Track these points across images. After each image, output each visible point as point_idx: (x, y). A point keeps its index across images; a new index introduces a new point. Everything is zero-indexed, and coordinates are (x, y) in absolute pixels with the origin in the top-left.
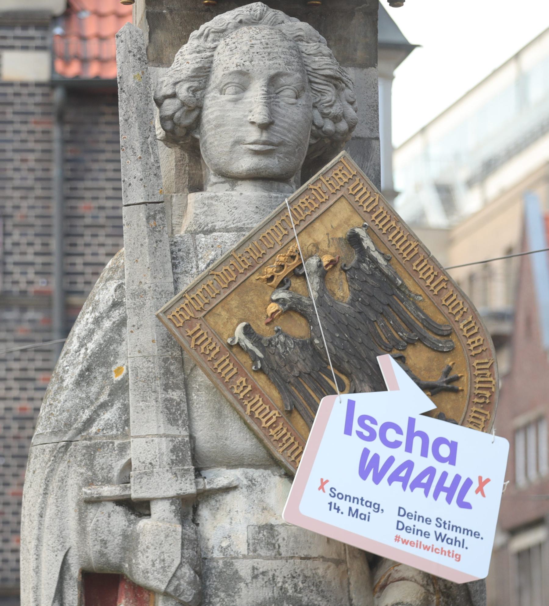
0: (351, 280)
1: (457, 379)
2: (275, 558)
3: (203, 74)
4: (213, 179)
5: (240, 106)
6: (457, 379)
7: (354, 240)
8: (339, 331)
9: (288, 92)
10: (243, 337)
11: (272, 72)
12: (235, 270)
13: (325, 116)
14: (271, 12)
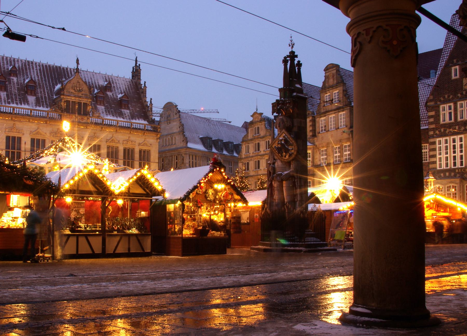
7: (284, 137)
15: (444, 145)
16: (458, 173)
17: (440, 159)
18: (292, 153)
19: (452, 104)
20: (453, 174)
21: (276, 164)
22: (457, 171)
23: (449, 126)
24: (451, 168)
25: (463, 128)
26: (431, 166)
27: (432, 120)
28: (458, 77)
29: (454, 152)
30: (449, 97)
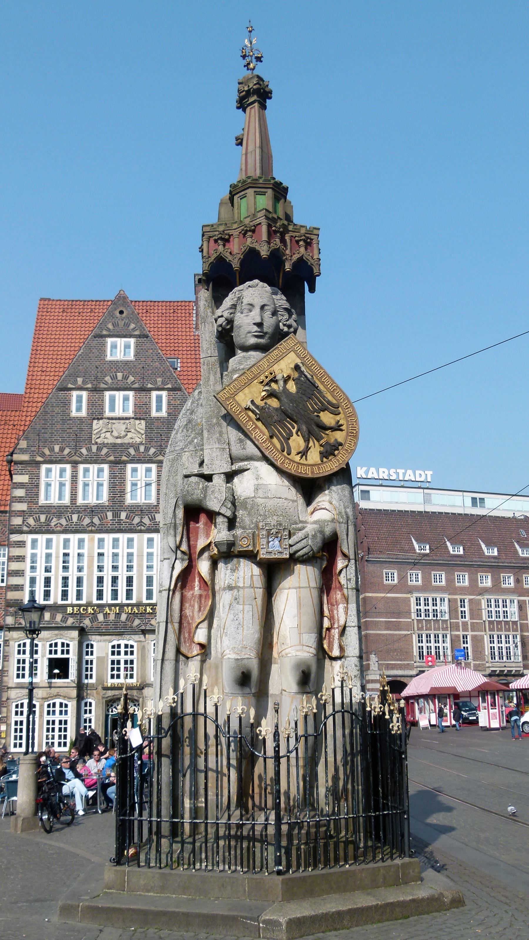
0: (296, 384)
1: (342, 425)
2: (266, 498)
3: (234, 306)
4: (239, 352)
5: (249, 317)
6: (342, 425)
7: (297, 368)
8: (292, 403)
9: (269, 313)
10: (251, 405)
11: (262, 304)
12: (247, 378)
13: (284, 325)
14: (261, 283)
15: (37, 551)
16: (72, 615)
17: (33, 581)
18: (337, 445)
19: (68, 467)
20: (59, 617)
21: (243, 486)
22: (69, 610)
23: (59, 511)
24: (55, 603)
25: (87, 521)
26: (12, 595)
27: (20, 493)
28: (84, 413)
29: (65, 568)
30: (62, 450)
